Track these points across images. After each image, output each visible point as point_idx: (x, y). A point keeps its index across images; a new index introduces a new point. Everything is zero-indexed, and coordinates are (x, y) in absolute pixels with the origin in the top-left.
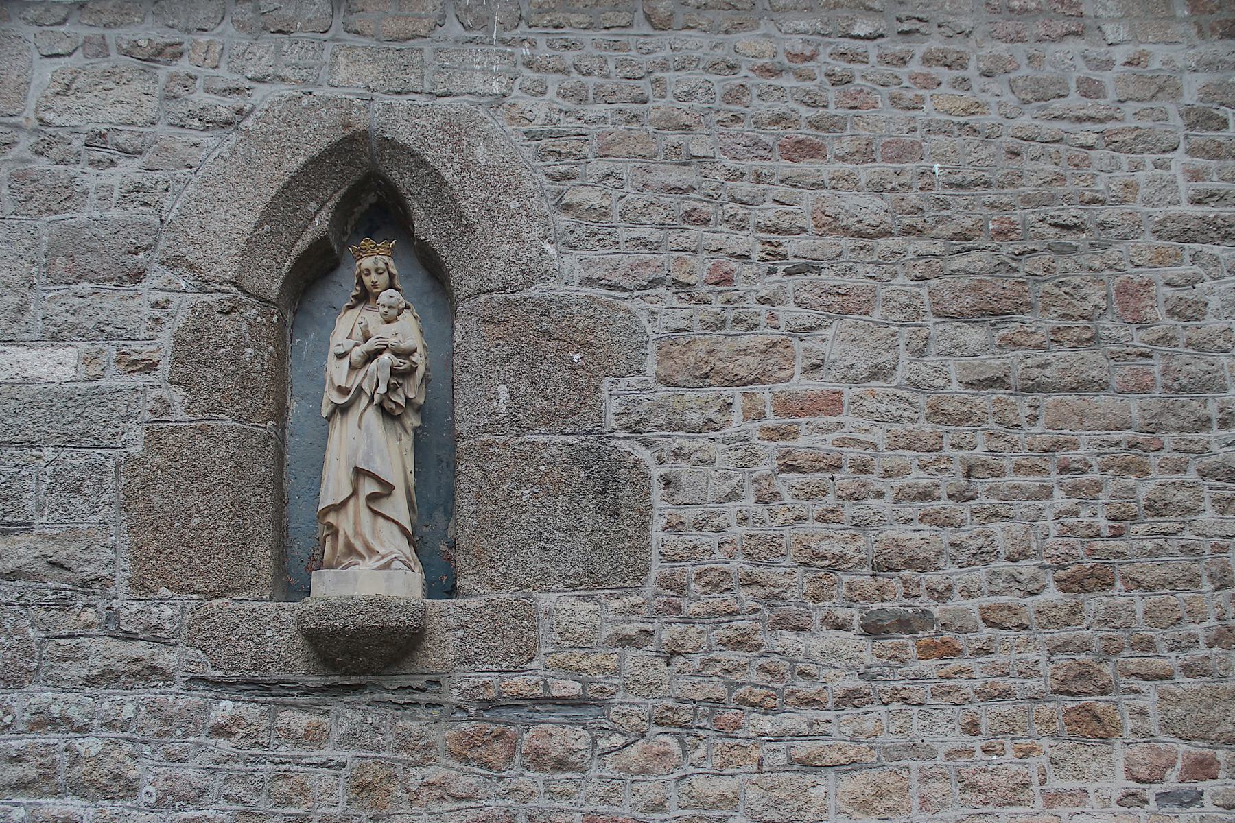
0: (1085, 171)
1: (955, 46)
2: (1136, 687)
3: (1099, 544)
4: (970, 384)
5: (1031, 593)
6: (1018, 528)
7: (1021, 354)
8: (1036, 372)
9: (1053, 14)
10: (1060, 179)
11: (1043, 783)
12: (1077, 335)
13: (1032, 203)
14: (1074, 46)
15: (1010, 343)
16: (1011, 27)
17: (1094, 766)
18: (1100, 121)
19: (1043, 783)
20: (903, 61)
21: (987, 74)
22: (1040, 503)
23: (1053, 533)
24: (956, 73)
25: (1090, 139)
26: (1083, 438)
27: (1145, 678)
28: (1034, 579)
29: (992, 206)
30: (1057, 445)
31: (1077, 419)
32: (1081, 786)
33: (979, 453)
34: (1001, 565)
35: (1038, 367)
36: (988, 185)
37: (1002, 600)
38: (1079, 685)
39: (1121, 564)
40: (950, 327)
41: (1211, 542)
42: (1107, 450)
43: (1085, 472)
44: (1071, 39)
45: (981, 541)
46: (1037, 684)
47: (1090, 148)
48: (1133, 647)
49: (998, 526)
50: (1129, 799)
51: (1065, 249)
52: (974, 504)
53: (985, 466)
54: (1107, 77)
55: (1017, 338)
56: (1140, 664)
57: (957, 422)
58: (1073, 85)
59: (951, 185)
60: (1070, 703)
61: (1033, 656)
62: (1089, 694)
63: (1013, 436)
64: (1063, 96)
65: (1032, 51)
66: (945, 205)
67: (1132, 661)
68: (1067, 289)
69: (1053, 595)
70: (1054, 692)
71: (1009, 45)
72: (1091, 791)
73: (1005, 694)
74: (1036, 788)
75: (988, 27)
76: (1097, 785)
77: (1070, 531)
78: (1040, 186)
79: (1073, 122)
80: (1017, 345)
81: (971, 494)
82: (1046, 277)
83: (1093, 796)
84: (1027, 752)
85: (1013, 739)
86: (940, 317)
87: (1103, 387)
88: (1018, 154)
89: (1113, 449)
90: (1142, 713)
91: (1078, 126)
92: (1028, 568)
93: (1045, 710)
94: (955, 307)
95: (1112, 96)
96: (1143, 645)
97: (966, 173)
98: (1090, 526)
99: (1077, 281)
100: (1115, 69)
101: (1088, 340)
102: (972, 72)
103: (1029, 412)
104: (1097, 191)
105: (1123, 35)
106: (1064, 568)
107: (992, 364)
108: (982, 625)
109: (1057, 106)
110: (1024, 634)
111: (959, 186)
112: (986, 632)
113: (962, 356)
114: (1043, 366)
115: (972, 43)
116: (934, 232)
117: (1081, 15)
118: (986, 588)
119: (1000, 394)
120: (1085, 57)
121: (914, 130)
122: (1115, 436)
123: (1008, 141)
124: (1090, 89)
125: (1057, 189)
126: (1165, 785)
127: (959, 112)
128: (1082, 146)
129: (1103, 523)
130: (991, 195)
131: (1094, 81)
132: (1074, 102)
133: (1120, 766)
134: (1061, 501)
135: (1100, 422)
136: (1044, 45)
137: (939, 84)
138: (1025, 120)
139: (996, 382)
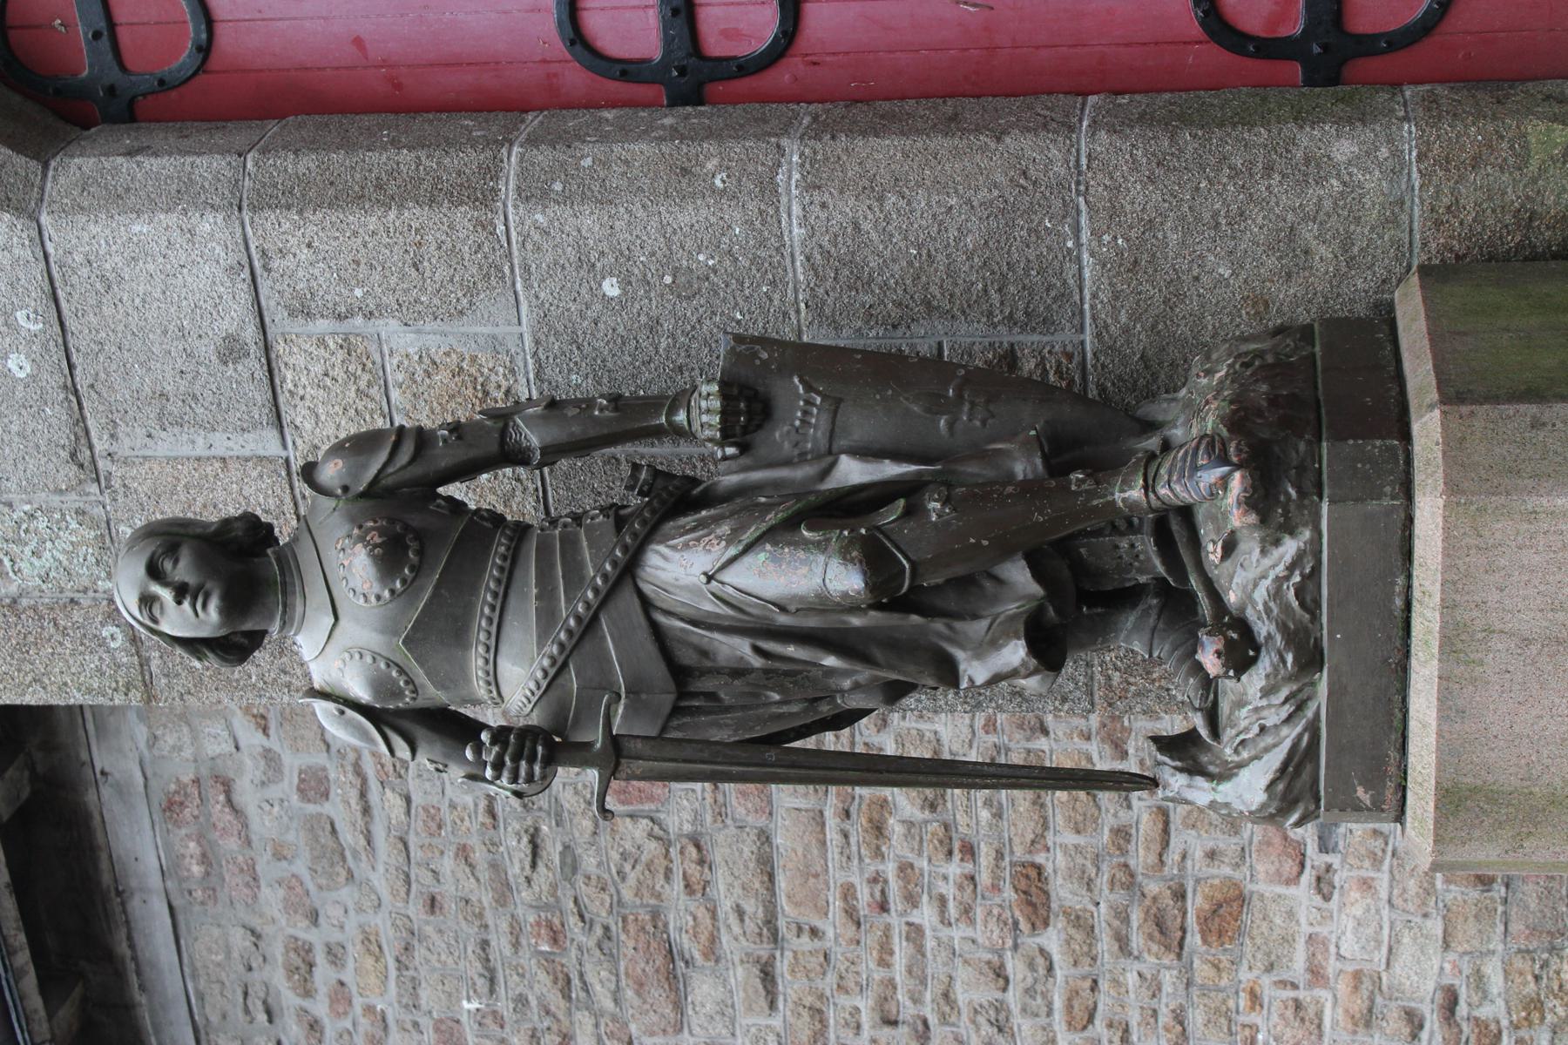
0: (448, 816)
1: (277, 951)
2: (1177, 857)
3: (984, 878)
4: (772, 1005)
5: (1050, 969)
6: (962, 974)
7: (725, 938)
8: (750, 926)
9: (202, 819)
10: (463, 852)
11: (1295, 986)
12: (693, 866)
13: (504, 892)
14: (246, 794)
15: (712, 951)
16: (233, 881)
17: (1278, 921)
18: (364, 781)
19: (1295, 986)
20: (314, 1026)
21: (314, 917)
22: (930, 944)
23: (969, 932)
24: (320, 958)
25: (394, 801)
26: (837, 876)
27: (1165, 843)
28: (1031, 966)
29: (516, 945)
30: (851, 914)
31: (812, 880)
32: (1303, 940)
33: (865, 1004)
34: (1013, 997)
35: (742, 921)
36: (485, 944)
37: (1058, 1003)
38: (1173, 925)
39: (1012, 852)
40: (695, 1019)
41: (980, 733)
42: (854, 848)
43: (886, 881)
44: (236, 798)
45: (981, 1020)
46: (1168, 979)
47: (408, 800)
48: (1124, 852)
49: (961, 996)
50: (1323, 885)
51: (569, 860)
52: (933, 1020)
53: (883, 1000)
54: (292, 763)
55: (703, 938)
56: (1148, 849)
57: (823, 1022)
58: (311, 808)
59: (492, 991)
60: (1194, 940)
61: (1131, 979)
62: (1185, 913)
63: (838, 954)
64: (332, 825)
65: (268, 855)
66: (522, 1001)
67: (1140, 857)
68: (627, 867)
69: (1052, 939)
70: (1179, 956)
71: (263, 883)
72: (1311, 930)
73: (1179, 1018)
74: (1301, 994)
75: (240, 907)
76: (1303, 921)
77: (967, 911)
78: (478, 880)
79: (371, 817)
80: (714, 939)
81: (919, 1023)
82: (613, 890)
83: (1317, 929)
84: (1255, 998)
85: (1238, 1012)
86: (681, 1029)
87: (765, 837)
88: (433, 900)
89: (853, 840)
90: (1212, 855)
91: (376, 812)
92: (1015, 967)
93: (1202, 971)
94: (668, 1010)
95: (319, 759)
96: (1122, 842)
97: (472, 973)
98: (961, 888)
99: (615, 856)
100: (276, 747)
101: (698, 847)
102: (314, 937)
103: (805, 938)
104: (476, 805)
105: (218, 728)
106: (1016, 923)
107: (741, 976)
108: (1089, 1033)
109: (350, 837)
110: (1104, 985)
111: (492, 981)
112: (1099, 1025)
113: (733, 1006)
114: (740, 913)
115: (268, 930)
116: (561, 1017)
117: (197, 781)
118: (1043, 1020)
119: (782, 967)
120: (263, 783)
121: (416, 1024)
122: (832, 835)
123: (416, 910)
124: (314, 786)
125: (479, 855)
126: (1309, 841)
127: (380, 966)
128: (408, 812)
129: (955, 869)
130: (501, 944)
131: (302, 781)
132: (340, 808)
133: (1280, 889)
134: (926, 915)
135: (816, 852)
136: (254, 838)
137: (342, 984)
138: (381, 881)
139: (767, 975)
